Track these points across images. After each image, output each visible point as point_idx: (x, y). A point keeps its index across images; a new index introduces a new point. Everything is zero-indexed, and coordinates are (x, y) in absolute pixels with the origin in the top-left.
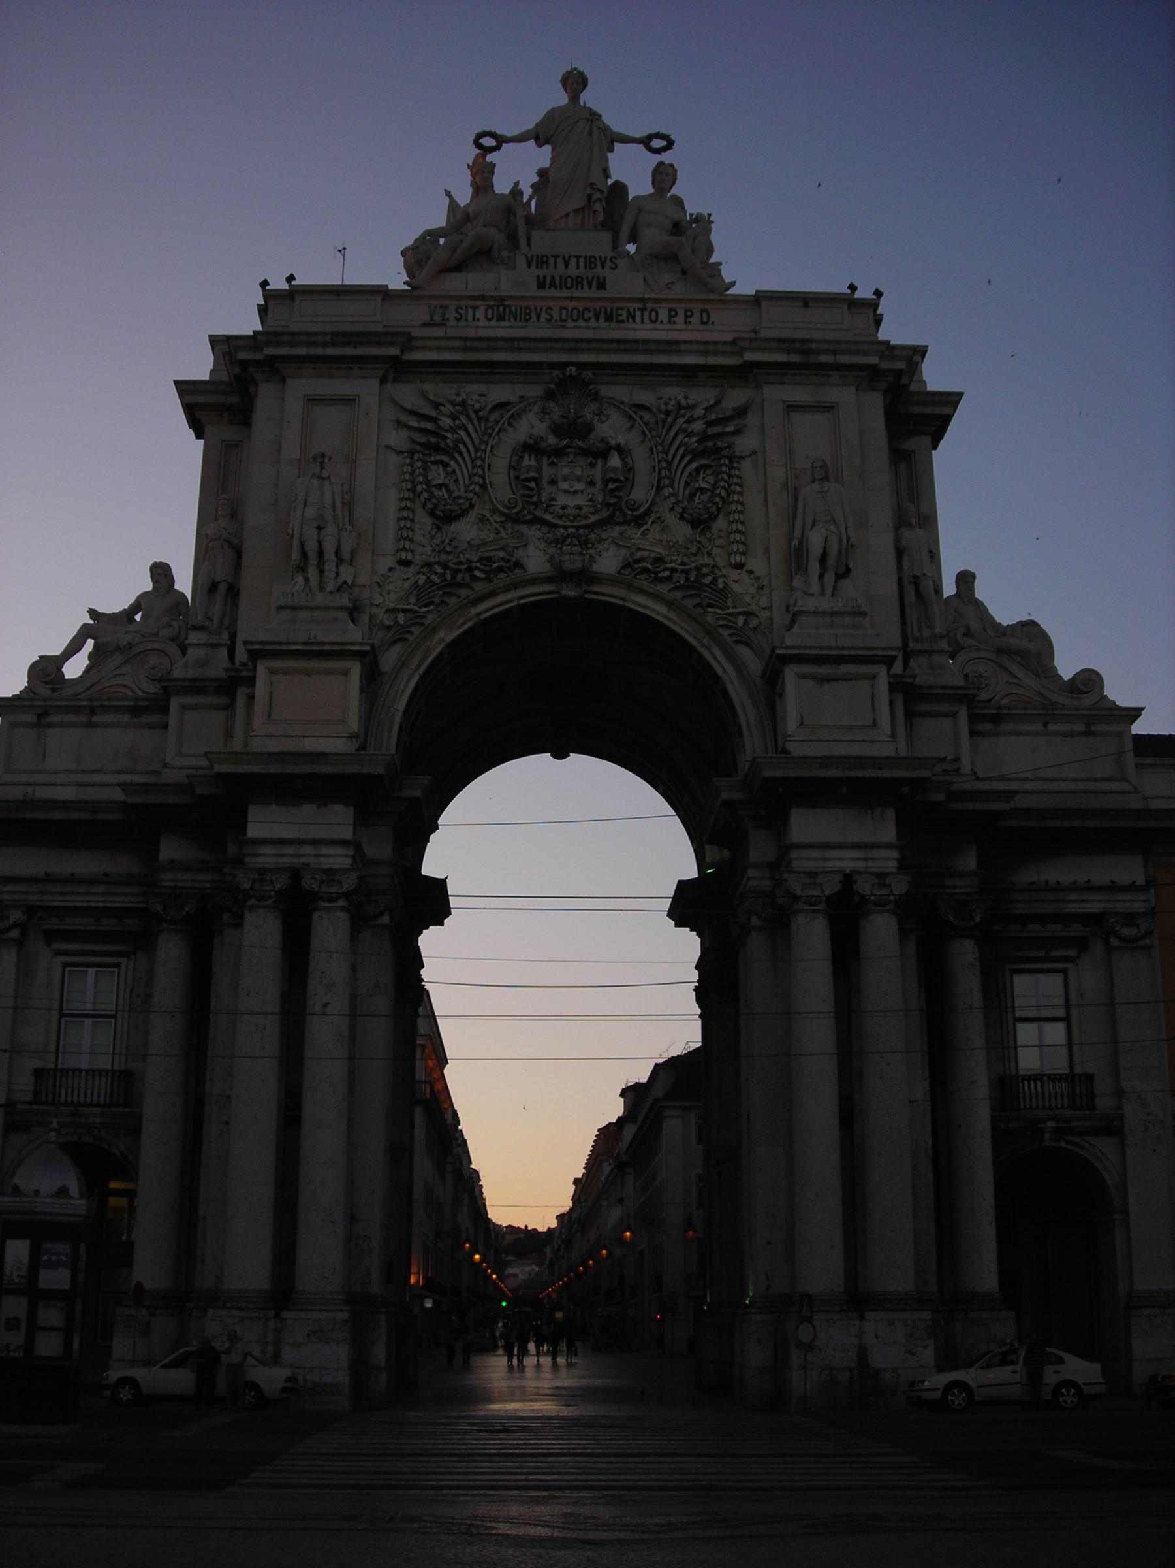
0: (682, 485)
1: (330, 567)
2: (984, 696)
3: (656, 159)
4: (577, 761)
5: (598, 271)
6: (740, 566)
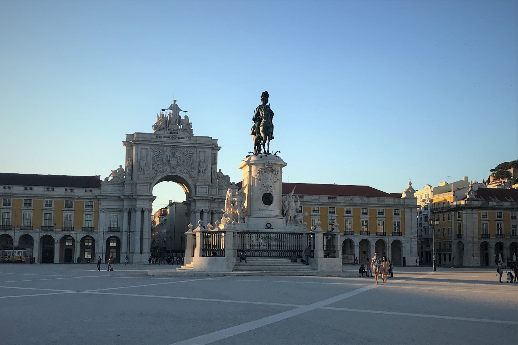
2: (221, 185)
4: (170, 181)
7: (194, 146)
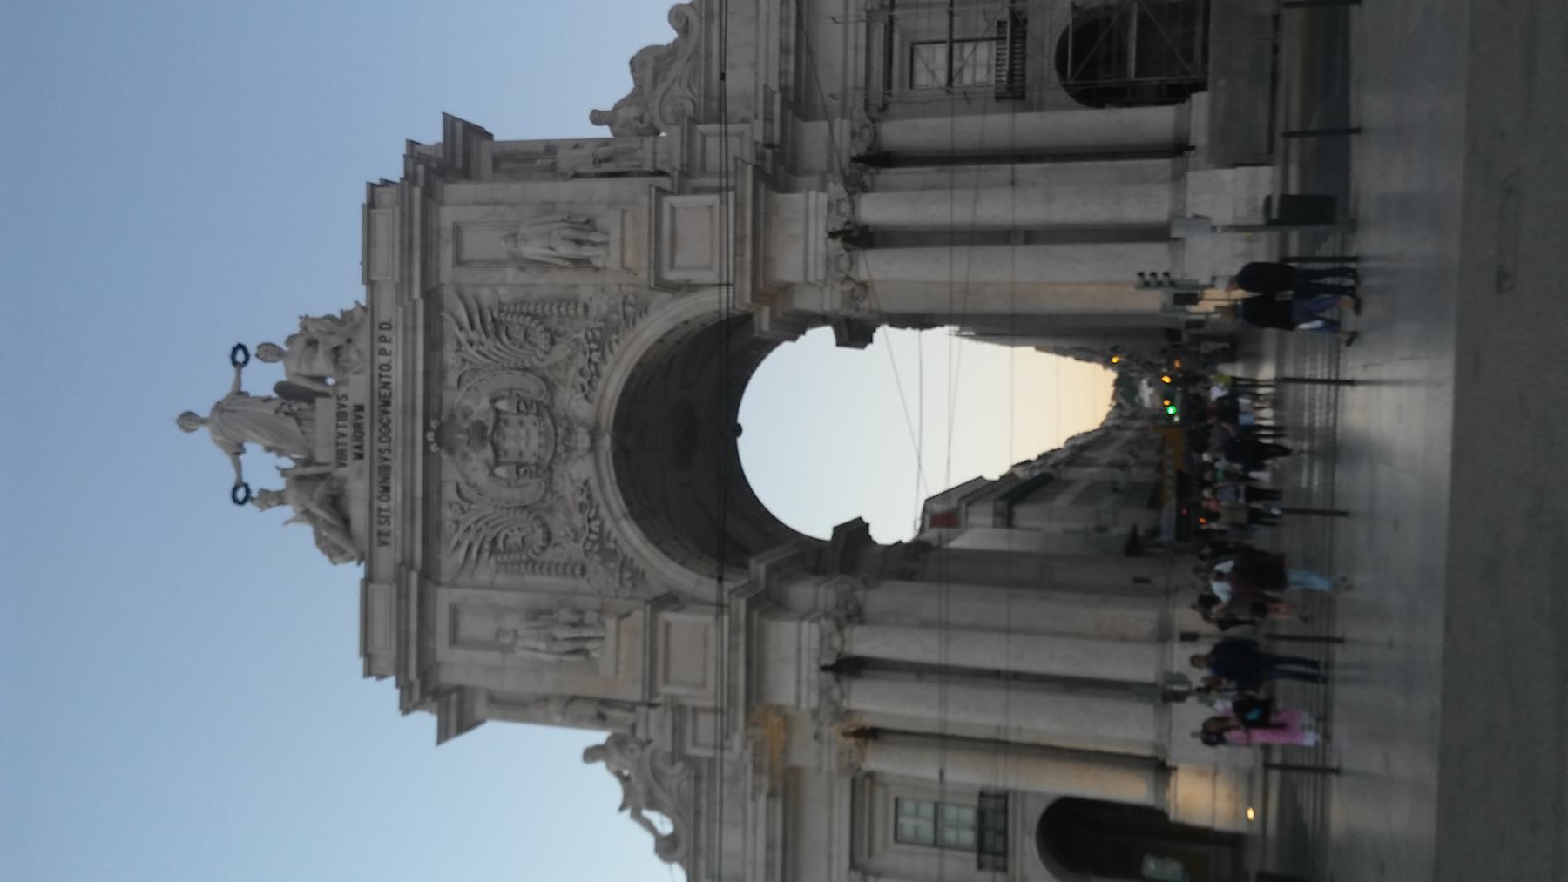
0: (521, 351)
1: (586, 633)
2: (689, 107)
3: (253, 361)
4: (743, 418)
5: (349, 410)
6: (586, 307)
7: (421, 305)
